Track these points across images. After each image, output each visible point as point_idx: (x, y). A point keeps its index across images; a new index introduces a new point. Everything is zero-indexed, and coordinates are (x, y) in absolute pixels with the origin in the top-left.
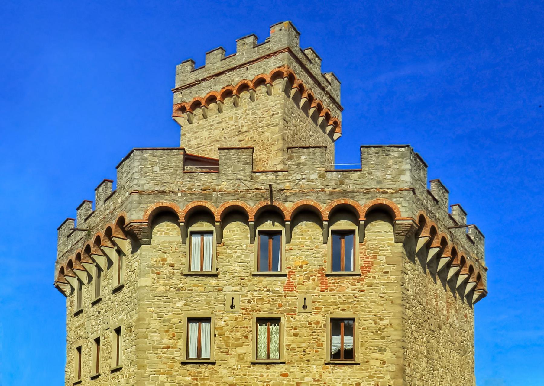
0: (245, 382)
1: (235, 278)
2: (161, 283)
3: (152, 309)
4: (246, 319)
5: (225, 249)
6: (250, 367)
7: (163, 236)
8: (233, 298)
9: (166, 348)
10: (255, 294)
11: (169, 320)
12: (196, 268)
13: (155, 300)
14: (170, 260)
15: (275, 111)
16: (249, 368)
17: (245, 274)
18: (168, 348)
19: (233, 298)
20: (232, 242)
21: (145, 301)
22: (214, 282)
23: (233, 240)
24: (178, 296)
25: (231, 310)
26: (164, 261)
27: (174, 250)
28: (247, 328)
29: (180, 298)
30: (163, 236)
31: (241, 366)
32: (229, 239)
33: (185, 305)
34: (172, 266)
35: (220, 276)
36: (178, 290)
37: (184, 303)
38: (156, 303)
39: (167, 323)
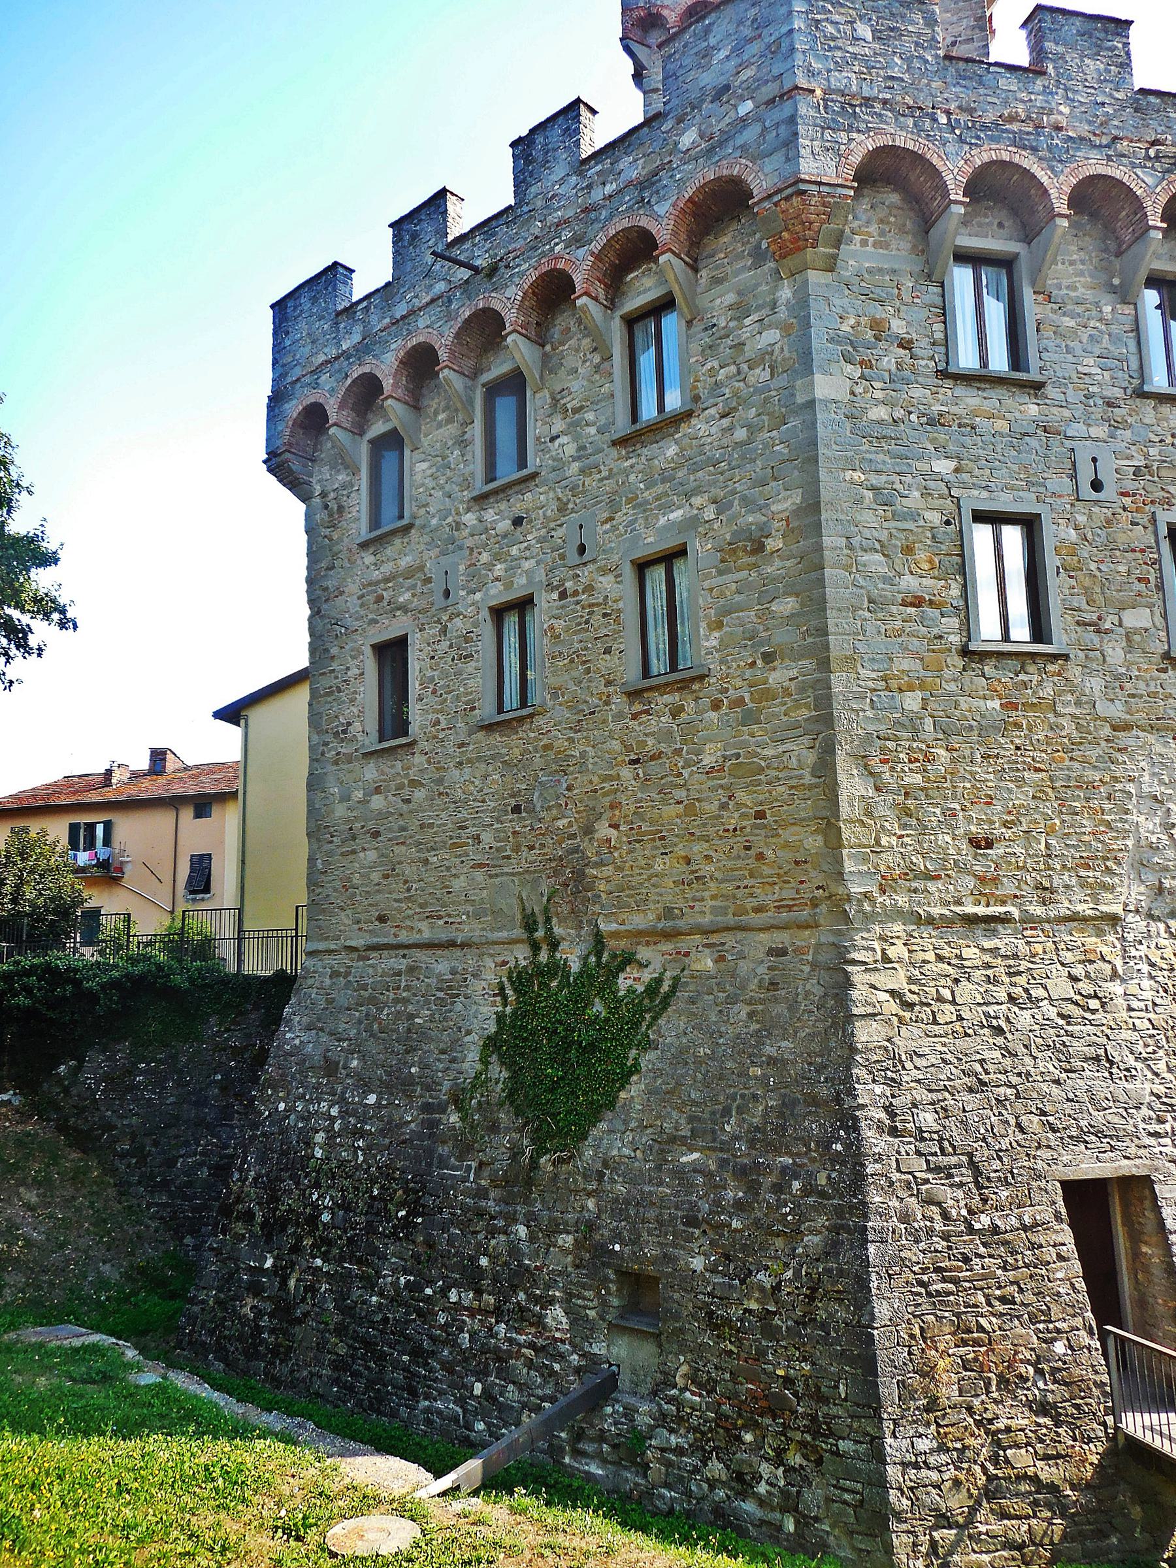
0: (1158, 719)
1: (1091, 402)
2: (879, 394)
3: (858, 476)
4: (1138, 524)
5: (1054, 311)
6: (1165, 671)
7: (869, 249)
8: (1094, 460)
9: (912, 605)
10: (1153, 452)
11: (914, 515)
12: (967, 359)
13: (865, 447)
14: (898, 327)
15: (960, 36)
16: (1163, 675)
17: (1118, 392)
18: (917, 602)
19: (1094, 460)
20: (1073, 294)
21: (834, 446)
22: (1033, 410)
23: (1075, 289)
24: (933, 441)
25: (1094, 495)
26: (879, 328)
27: (907, 298)
28: (1142, 551)
29: (941, 451)
30: (869, 249)
31: (1139, 669)
32: (1065, 283)
33: (957, 470)
34: (906, 345)
35: (1050, 391)
36: (932, 422)
37: (952, 465)
38: (868, 456)
39: (910, 525)
